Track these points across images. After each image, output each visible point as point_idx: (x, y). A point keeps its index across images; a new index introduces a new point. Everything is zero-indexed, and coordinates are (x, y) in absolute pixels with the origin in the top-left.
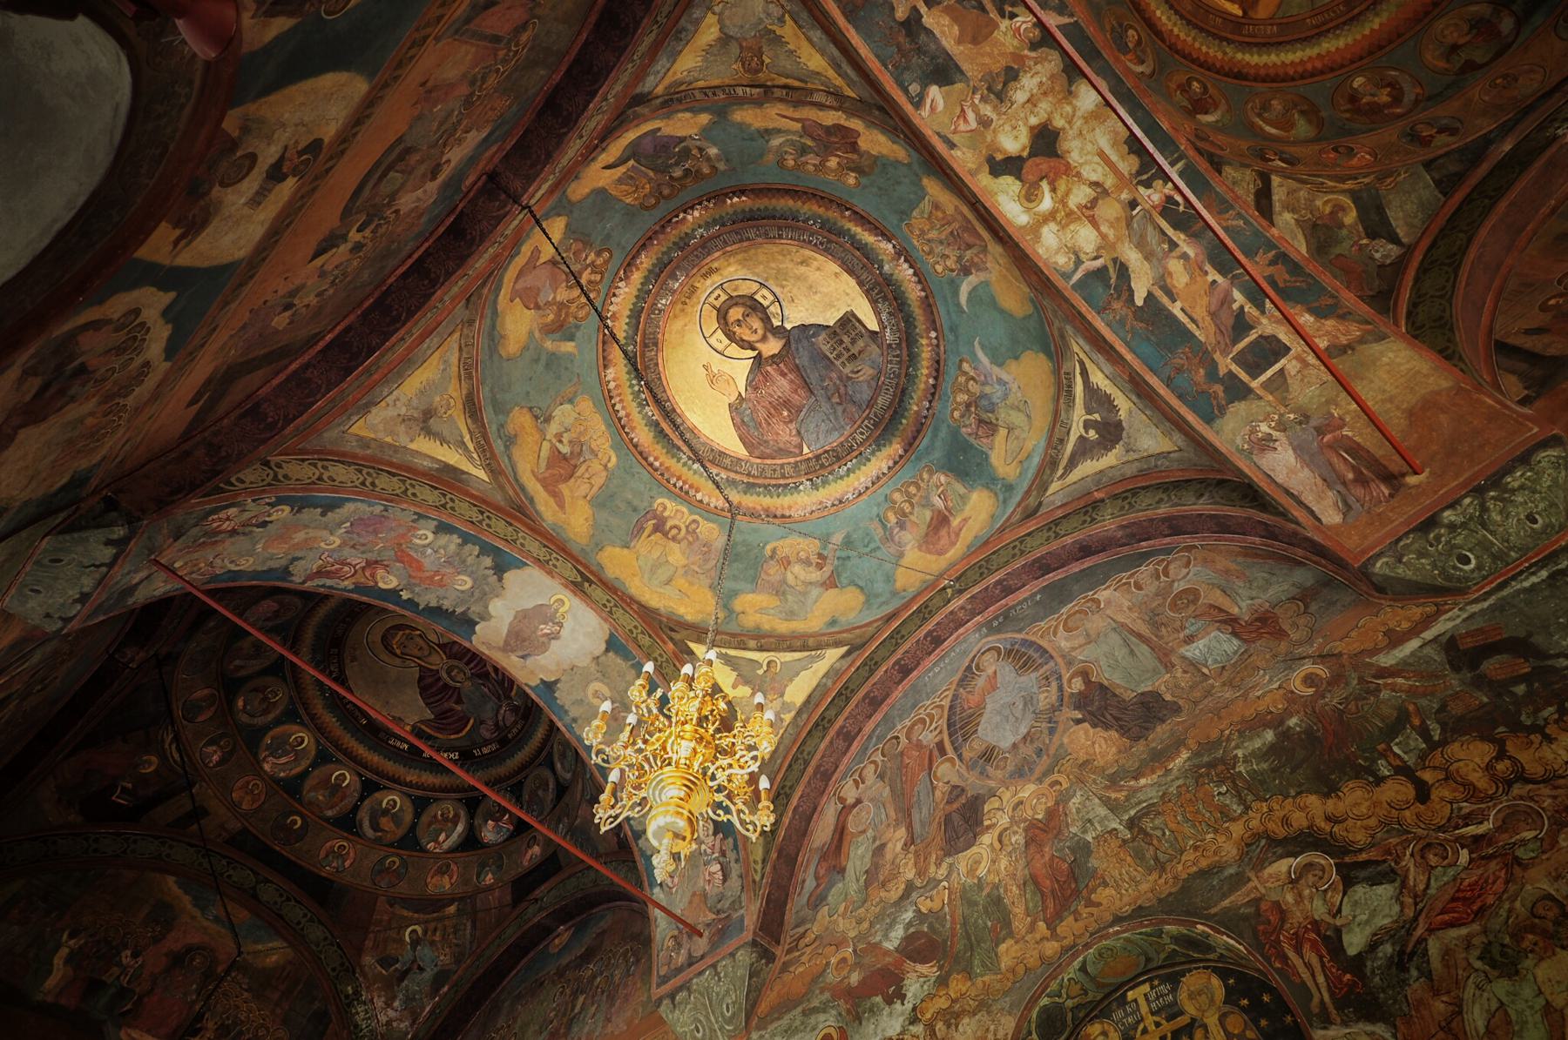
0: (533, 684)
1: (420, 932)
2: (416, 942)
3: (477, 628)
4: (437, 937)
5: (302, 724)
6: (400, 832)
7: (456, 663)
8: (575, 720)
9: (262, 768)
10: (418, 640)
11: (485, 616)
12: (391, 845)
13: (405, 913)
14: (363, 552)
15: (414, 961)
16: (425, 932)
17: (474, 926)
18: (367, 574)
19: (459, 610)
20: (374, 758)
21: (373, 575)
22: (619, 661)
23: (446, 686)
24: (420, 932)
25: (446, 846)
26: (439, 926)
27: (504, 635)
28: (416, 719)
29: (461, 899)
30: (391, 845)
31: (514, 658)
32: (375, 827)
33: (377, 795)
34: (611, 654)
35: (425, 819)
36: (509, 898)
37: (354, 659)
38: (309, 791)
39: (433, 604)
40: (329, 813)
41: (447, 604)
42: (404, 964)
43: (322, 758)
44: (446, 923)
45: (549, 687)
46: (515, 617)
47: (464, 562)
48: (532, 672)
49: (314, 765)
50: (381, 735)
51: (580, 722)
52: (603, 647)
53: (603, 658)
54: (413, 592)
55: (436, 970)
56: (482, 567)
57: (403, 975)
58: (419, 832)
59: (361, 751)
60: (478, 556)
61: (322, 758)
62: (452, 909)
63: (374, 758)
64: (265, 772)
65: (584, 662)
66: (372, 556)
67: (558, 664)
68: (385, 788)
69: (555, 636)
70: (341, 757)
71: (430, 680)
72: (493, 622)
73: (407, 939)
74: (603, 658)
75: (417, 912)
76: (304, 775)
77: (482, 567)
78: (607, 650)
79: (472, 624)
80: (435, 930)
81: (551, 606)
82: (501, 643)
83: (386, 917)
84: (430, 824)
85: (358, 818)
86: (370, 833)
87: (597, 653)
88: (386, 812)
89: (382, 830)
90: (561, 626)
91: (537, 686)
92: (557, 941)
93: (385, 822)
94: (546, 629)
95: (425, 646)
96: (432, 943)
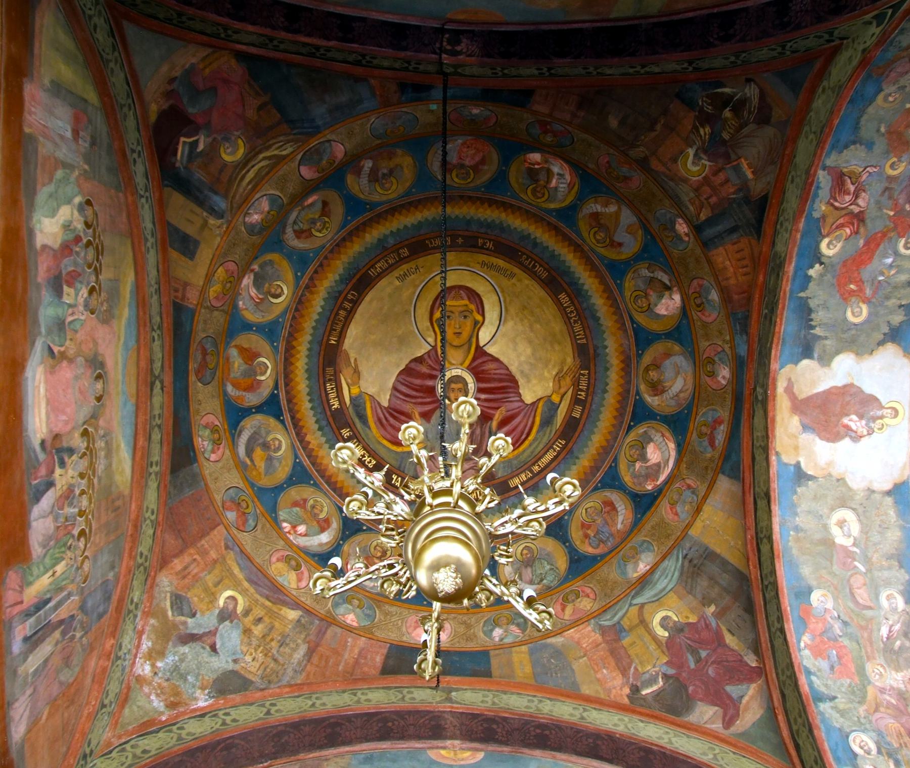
0: (785, 459)
1: (240, 609)
2: (226, 615)
3: (805, 362)
4: (258, 630)
5: (297, 279)
6: (266, 482)
7: (470, 379)
8: (797, 529)
9: (244, 277)
10: (469, 323)
11: (826, 360)
12: (252, 485)
13: (236, 571)
14: (878, 202)
15: (213, 633)
16: (247, 612)
17: (311, 652)
18: (841, 221)
19: (818, 331)
20: (302, 385)
21: (841, 226)
22: (892, 513)
23: (432, 390)
24: (240, 609)
25: (302, 542)
26: (266, 619)
27: (815, 391)
28: (371, 390)
29: (308, 612)
30: (252, 485)
31: (795, 421)
32: (249, 452)
33: (272, 421)
34: (889, 500)
35: (294, 493)
36: (379, 659)
37: (402, 278)
38: (236, 346)
39: (812, 304)
40: (230, 388)
41: (819, 316)
42: (200, 626)
43: (269, 331)
44: (277, 624)
45: (800, 476)
46: (845, 386)
47: (887, 298)
48: (796, 448)
49: (260, 329)
50: (330, 370)
51: (801, 535)
52: (888, 486)
53: (877, 496)
54: (822, 275)
55: (231, 666)
56: (890, 318)
57: (190, 638)
58: (284, 499)
59: (301, 364)
60: (901, 306)
61: (269, 331)
62: (293, 615)
63: (302, 385)
64: (241, 282)
65: (856, 483)
66: (872, 213)
67: (830, 464)
68: (283, 422)
69: (857, 438)
70: (282, 347)
71: (424, 369)
72: (821, 371)
73: (221, 602)
74: (877, 496)
75: (250, 581)
76: (248, 327)
77: (890, 318)
78: (889, 493)
79: (807, 352)
80: (259, 620)
81: (882, 407)
82: (802, 396)
83: (213, 554)
84: (295, 504)
85: (242, 423)
86: (242, 450)
87: (877, 486)
88: (266, 446)
89: (252, 461)
90: (870, 432)
91: (786, 465)
92: (443, 752)
93: (258, 453)
94: (853, 422)
95: (465, 335)
96: (247, 632)
